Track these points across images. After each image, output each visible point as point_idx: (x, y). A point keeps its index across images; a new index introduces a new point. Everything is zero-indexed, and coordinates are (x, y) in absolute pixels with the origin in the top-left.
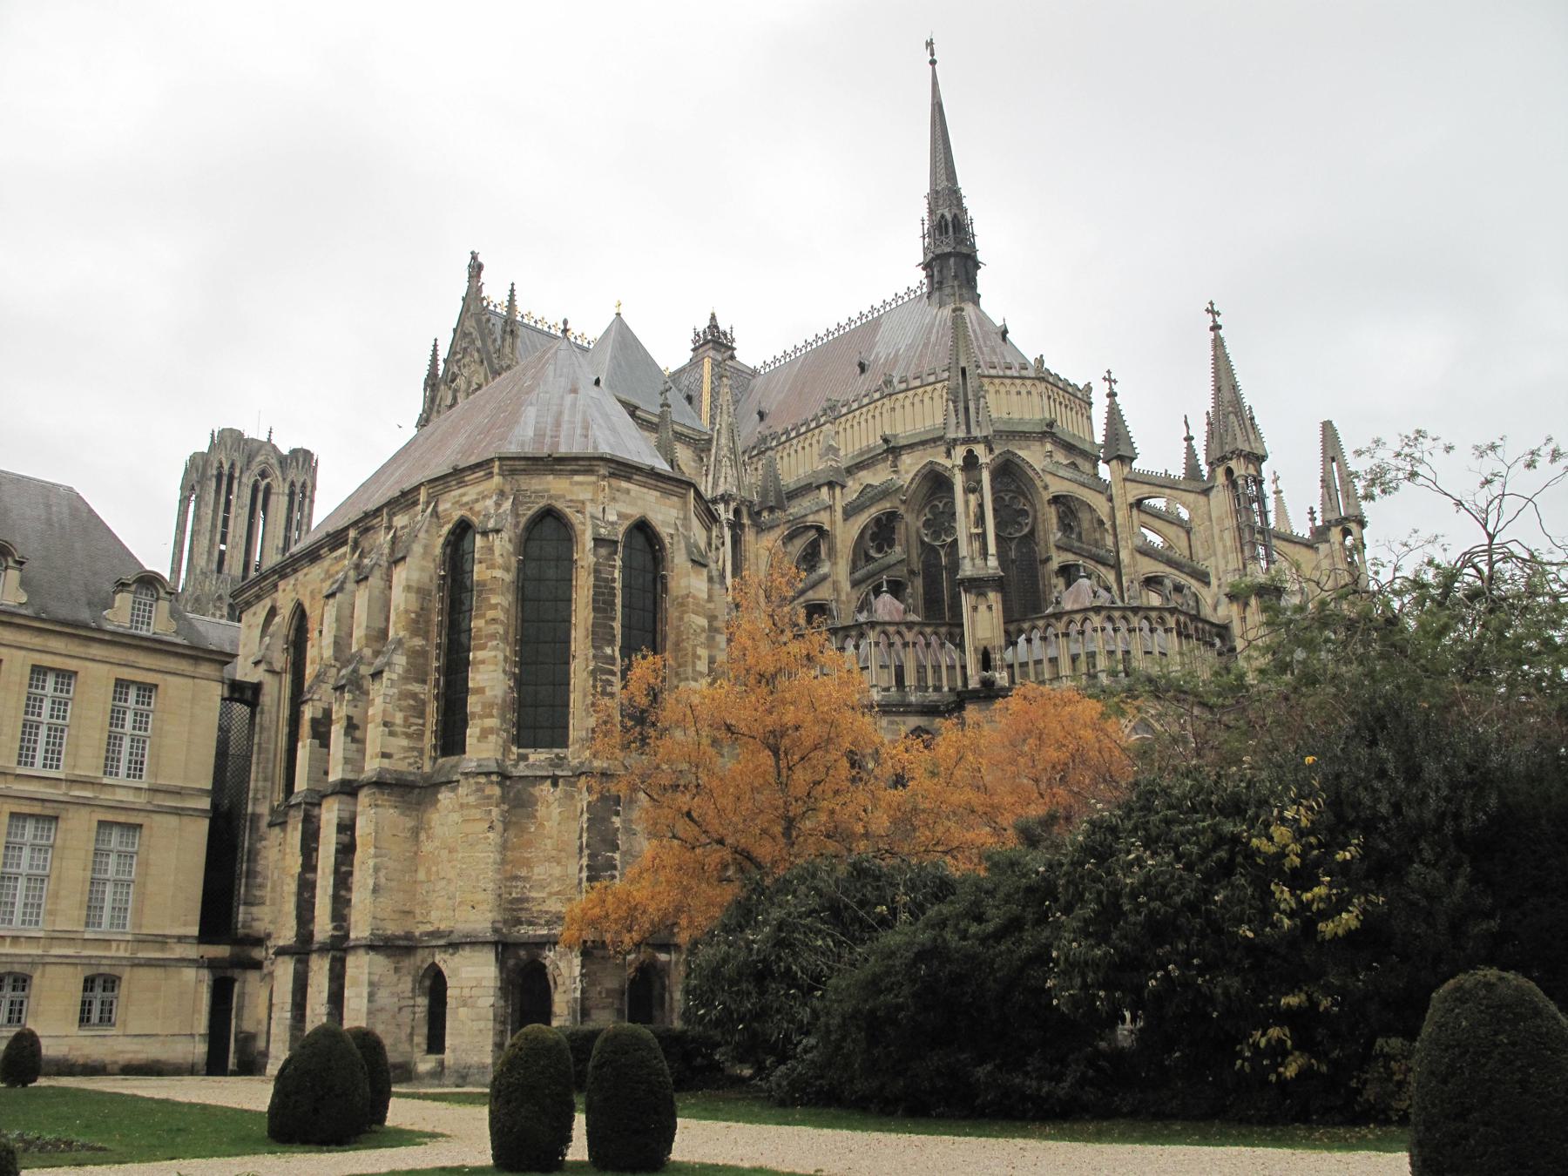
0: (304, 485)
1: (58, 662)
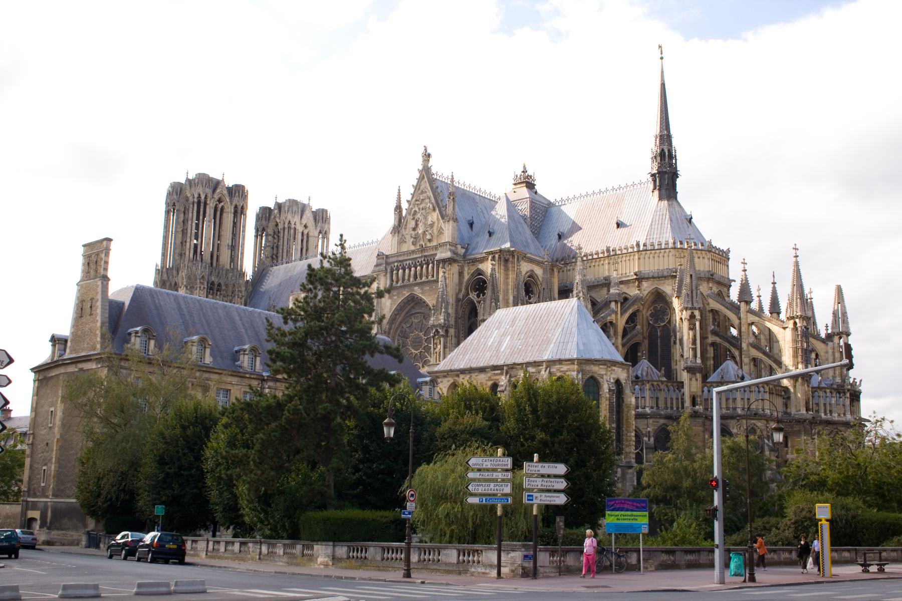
0: (242, 206)
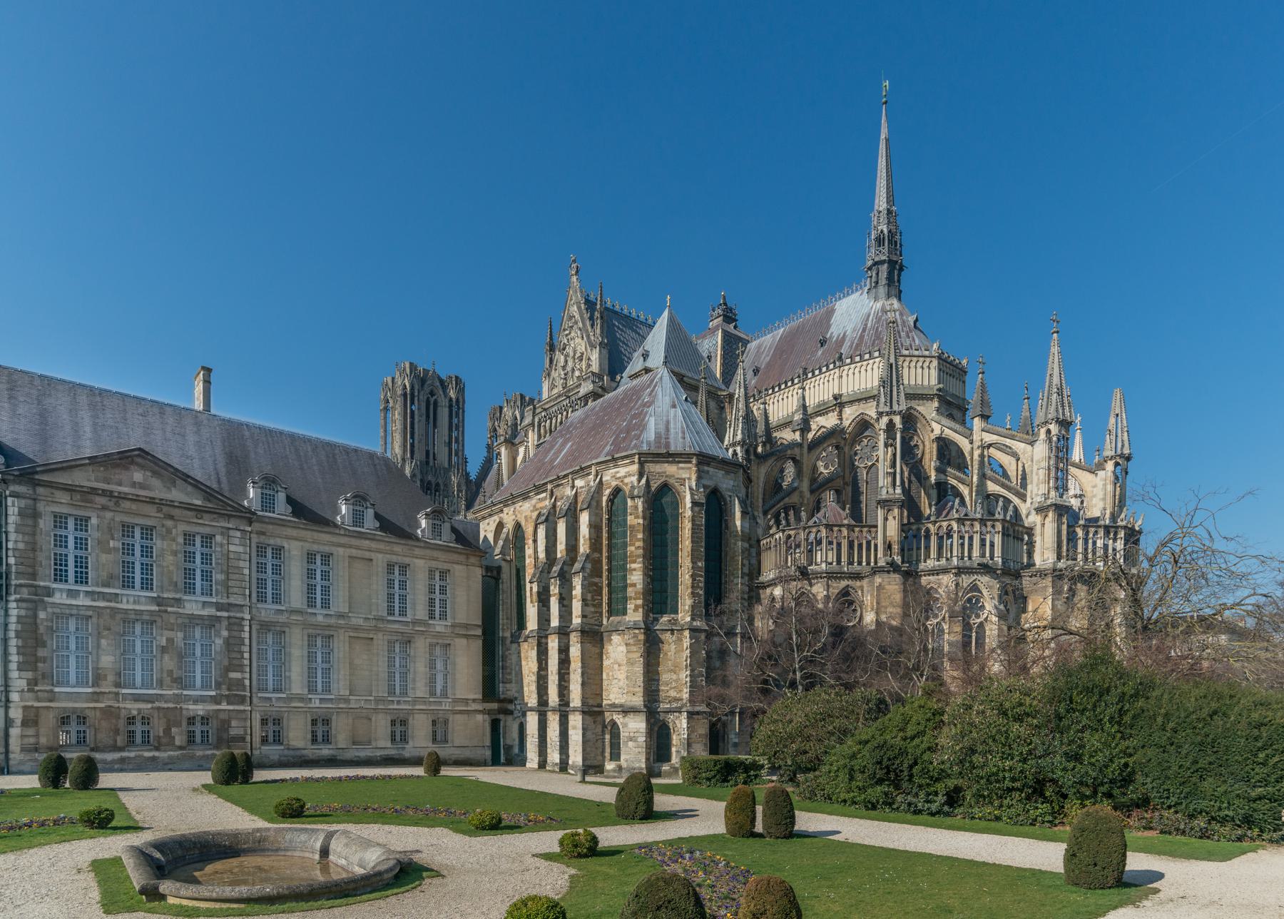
1: (400, 559)
